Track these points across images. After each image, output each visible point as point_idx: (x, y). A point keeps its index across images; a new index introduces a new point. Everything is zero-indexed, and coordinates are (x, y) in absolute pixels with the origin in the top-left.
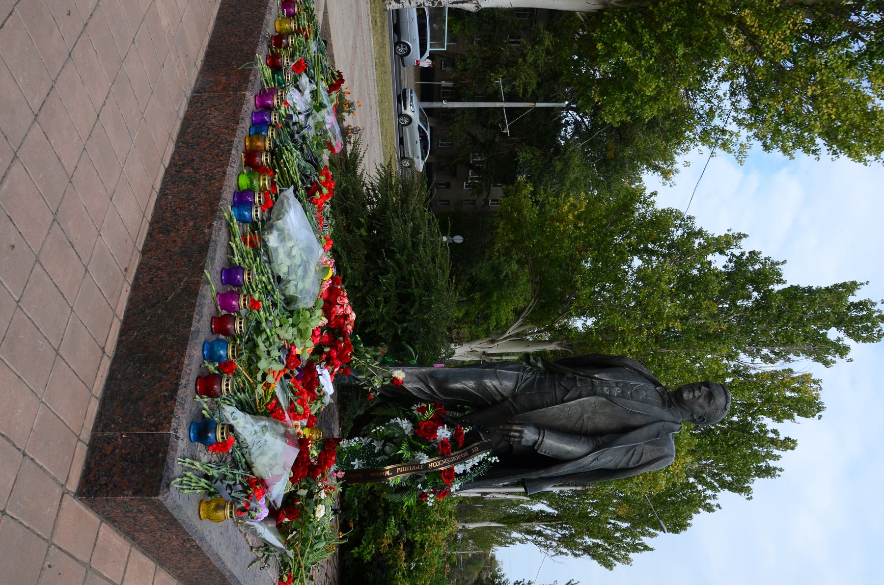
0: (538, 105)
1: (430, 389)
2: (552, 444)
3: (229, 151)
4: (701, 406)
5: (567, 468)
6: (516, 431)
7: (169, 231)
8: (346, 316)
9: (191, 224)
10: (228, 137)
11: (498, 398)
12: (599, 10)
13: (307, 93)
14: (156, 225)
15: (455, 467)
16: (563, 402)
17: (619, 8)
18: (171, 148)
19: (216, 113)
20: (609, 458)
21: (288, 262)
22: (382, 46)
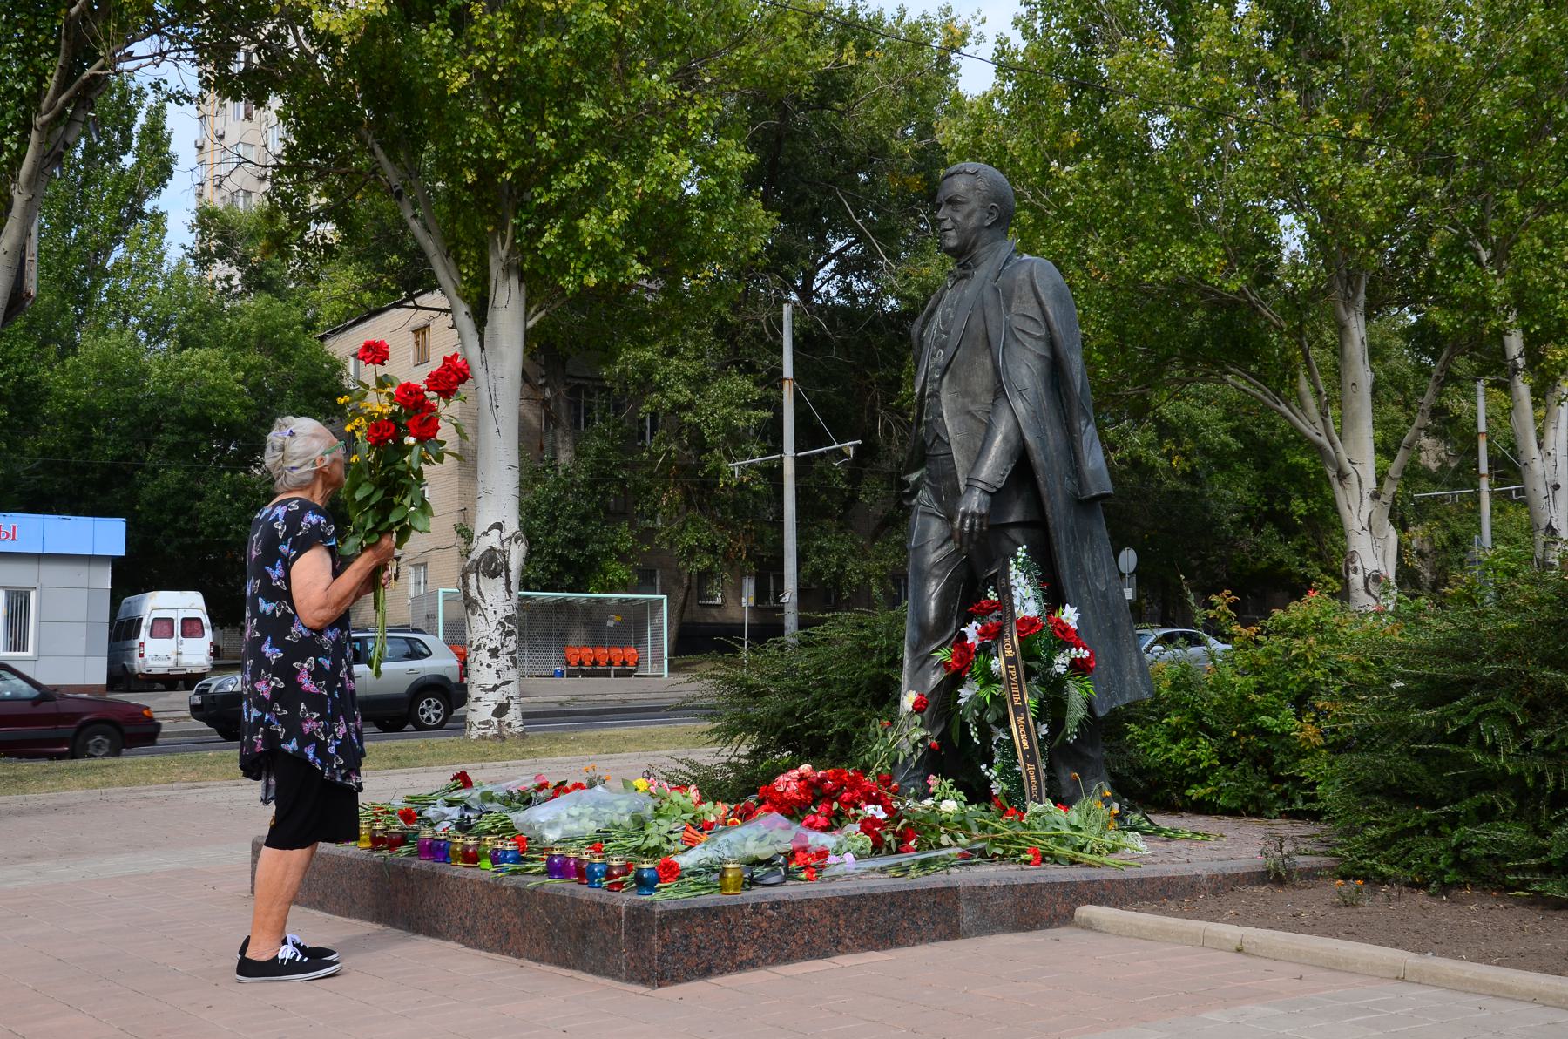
0: (788, 371)
4: (969, 215)
6: (963, 522)
8: (802, 777)
12: (521, 281)
13: (446, 810)
15: (1020, 613)
17: (513, 240)
18: (451, 944)
21: (585, 821)
22: (578, 739)
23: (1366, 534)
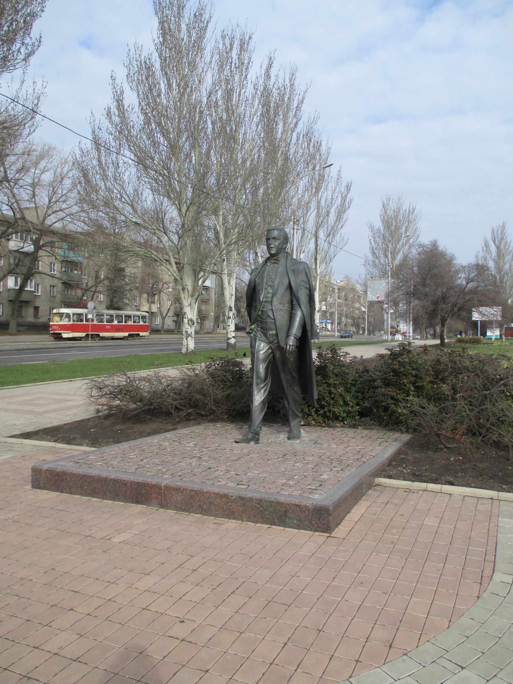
1: (264, 386)
2: (296, 330)
3: (195, 491)
5: (308, 321)
7: (234, 512)
9: (230, 503)
10: (188, 492)
11: (270, 351)
14: (231, 517)
16: (274, 319)
19: (174, 497)
20: (303, 296)
23: (189, 307)
